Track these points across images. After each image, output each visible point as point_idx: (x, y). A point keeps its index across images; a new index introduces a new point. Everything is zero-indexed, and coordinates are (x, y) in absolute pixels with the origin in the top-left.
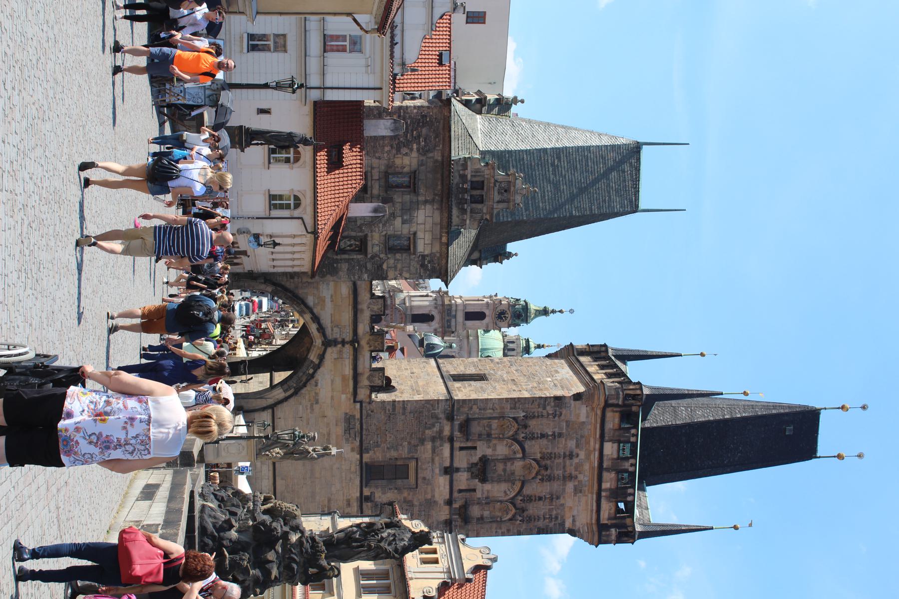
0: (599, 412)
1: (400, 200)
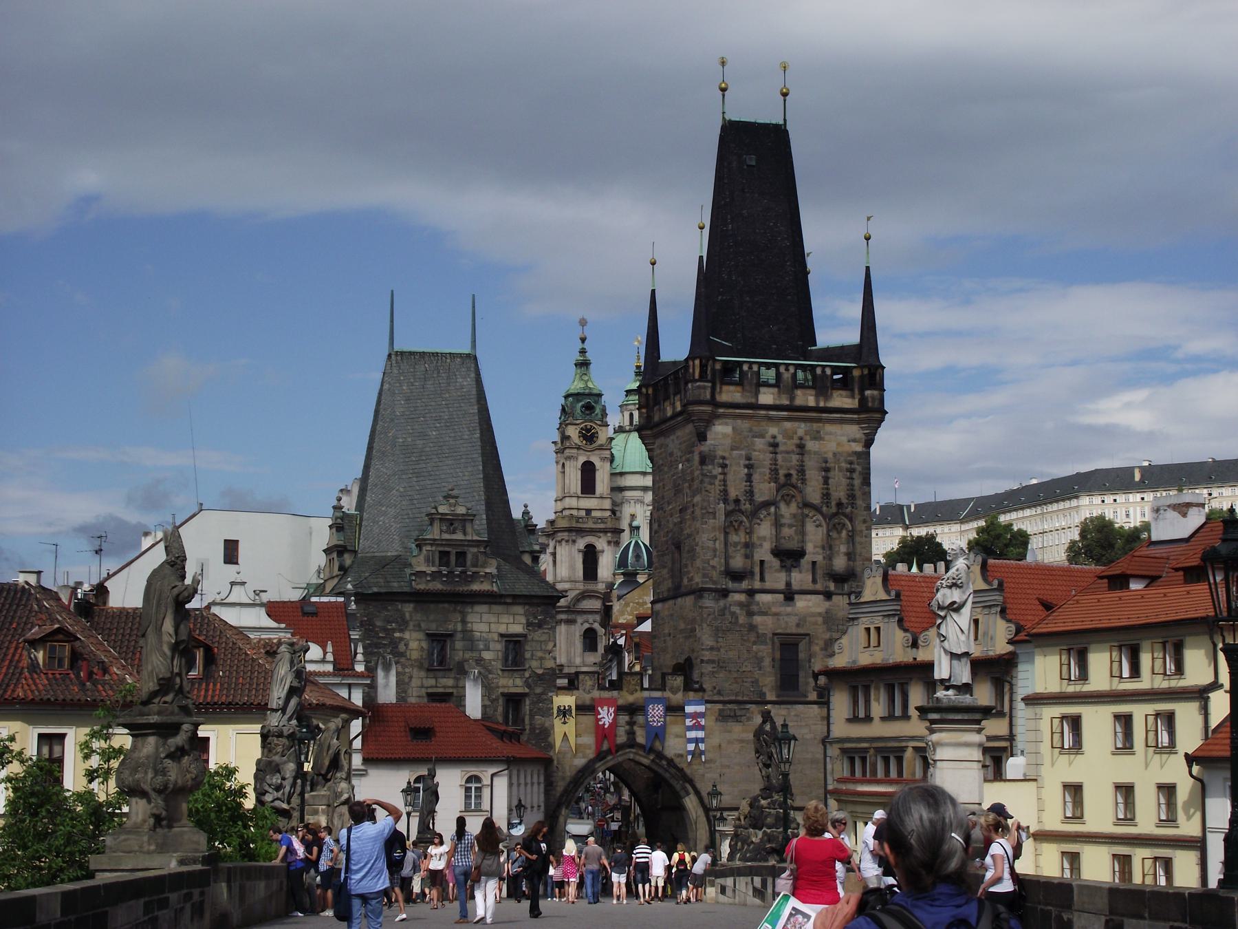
0: (721, 410)
1: (461, 653)
